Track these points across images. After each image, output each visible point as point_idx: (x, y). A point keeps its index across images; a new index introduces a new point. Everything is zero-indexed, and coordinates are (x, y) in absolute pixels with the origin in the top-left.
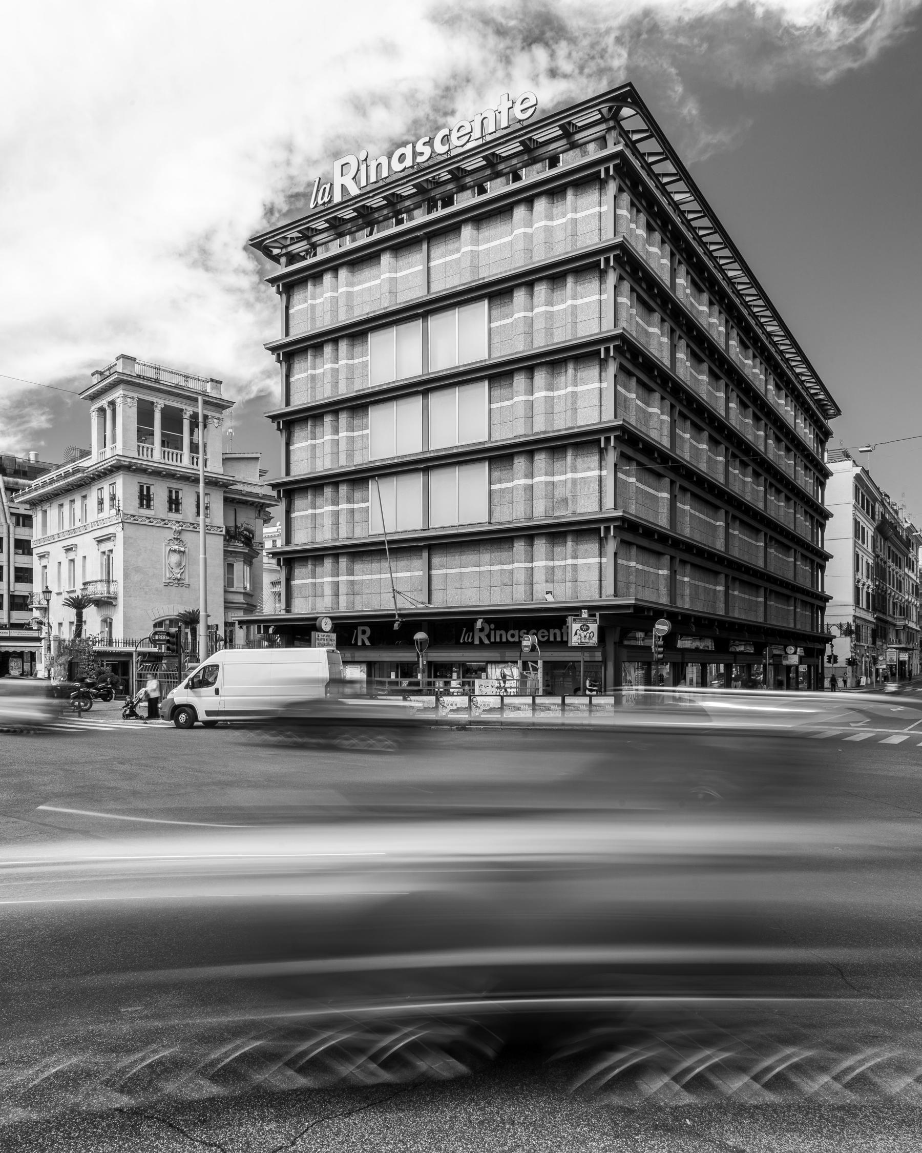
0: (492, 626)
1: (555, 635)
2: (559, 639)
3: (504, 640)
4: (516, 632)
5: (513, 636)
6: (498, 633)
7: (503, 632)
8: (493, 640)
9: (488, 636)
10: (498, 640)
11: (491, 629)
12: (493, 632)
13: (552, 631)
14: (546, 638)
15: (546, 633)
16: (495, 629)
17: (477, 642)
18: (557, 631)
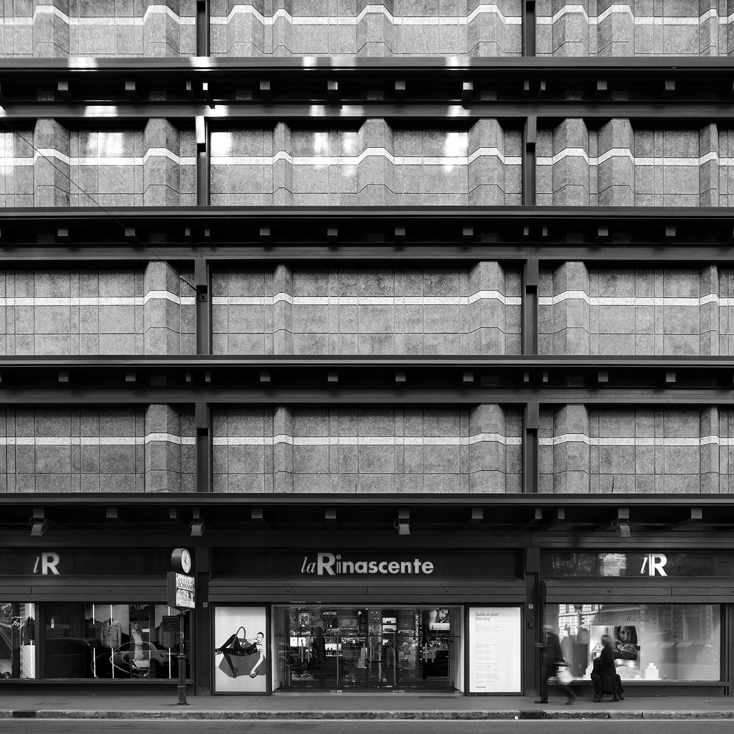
0: (339, 557)
1: (406, 567)
2: (410, 571)
3: (352, 571)
4: (365, 564)
5: (361, 567)
6: (345, 564)
7: (351, 564)
8: (339, 571)
9: (334, 567)
10: (345, 571)
11: (337, 560)
12: (339, 564)
13: (403, 564)
14: (397, 571)
15: (397, 566)
16: (342, 561)
17: (320, 572)
18: (409, 564)
